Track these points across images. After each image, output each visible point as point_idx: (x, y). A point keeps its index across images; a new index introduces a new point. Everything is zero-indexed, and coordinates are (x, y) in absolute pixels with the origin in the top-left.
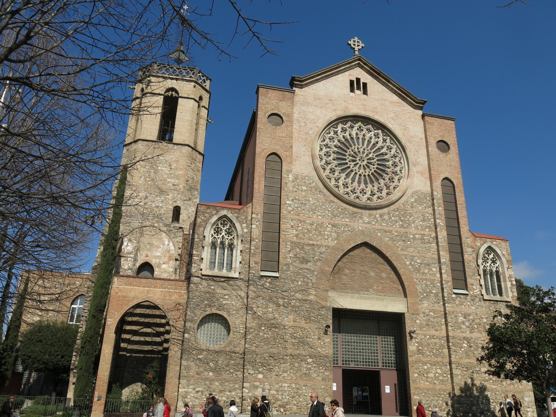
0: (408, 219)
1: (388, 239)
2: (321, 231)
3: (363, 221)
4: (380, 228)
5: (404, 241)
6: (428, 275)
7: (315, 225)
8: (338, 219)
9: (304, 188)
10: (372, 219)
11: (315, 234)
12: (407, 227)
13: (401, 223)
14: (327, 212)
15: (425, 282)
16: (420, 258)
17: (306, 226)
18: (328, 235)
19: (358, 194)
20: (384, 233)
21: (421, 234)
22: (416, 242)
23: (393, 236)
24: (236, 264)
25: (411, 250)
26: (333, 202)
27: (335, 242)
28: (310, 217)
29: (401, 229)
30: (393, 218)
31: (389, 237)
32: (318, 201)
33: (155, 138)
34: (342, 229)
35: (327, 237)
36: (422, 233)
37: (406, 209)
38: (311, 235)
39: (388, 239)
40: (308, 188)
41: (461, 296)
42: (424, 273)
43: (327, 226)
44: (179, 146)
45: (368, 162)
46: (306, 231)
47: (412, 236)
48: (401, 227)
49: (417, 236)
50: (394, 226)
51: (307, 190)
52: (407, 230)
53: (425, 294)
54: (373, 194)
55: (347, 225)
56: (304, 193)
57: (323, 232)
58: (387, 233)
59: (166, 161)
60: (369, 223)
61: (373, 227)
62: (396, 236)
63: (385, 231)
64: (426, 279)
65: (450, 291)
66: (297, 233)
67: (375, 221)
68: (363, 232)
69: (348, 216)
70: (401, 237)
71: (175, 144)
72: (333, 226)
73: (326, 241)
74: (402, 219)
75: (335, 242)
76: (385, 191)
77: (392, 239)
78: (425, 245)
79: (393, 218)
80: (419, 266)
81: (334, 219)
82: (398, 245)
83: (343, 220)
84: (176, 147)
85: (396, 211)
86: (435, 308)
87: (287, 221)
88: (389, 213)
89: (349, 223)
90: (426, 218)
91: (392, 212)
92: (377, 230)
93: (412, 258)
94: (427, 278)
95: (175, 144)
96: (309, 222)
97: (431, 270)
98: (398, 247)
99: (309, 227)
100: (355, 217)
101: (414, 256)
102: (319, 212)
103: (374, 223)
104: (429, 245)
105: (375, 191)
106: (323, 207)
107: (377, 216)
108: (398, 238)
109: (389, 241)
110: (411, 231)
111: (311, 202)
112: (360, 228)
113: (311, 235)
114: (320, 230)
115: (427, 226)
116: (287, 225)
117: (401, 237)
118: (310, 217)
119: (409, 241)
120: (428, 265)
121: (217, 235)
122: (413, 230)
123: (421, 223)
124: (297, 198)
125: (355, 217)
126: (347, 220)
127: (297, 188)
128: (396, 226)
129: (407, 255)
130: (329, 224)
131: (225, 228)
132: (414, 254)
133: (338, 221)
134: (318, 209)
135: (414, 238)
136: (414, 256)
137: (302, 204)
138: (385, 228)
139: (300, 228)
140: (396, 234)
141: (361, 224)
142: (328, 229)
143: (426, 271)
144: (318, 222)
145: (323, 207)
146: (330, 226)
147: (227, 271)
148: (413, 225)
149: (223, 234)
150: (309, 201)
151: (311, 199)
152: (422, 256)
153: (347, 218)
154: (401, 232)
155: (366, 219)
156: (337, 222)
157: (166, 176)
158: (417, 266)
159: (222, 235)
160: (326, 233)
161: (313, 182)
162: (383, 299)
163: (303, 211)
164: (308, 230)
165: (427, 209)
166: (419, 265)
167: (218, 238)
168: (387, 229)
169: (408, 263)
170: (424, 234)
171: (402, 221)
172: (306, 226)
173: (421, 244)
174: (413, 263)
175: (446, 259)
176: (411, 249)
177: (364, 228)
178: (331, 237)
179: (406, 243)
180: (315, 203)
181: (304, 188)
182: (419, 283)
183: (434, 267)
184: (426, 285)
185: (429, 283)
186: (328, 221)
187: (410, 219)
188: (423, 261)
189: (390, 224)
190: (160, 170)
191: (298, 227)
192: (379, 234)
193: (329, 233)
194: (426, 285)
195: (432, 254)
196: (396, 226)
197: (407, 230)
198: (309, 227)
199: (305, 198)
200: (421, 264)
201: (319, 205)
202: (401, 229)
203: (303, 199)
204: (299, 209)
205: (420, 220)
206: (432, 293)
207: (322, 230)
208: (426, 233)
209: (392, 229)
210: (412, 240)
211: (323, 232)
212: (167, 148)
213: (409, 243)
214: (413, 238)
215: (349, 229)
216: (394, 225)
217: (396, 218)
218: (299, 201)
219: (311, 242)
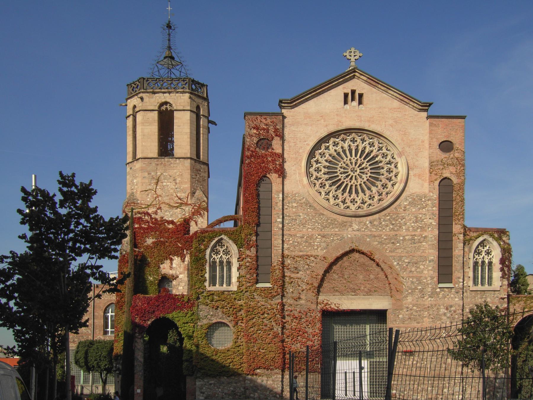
0: (400, 222)
1: (377, 243)
2: (310, 243)
3: (353, 229)
4: (369, 233)
5: (393, 243)
6: (415, 273)
7: (305, 237)
8: (327, 230)
9: (295, 205)
10: (361, 226)
11: (305, 246)
12: (398, 230)
13: (391, 227)
14: (317, 224)
15: (411, 279)
16: (408, 257)
17: (297, 240)
18: (317, 245)
19: (349, 204)
20: (373, 238)
21: (411, 235)
22: (405, 243)
23: (383, 239)
24: (234, 279)
25: (399, 251)
26: (323, 214)
27: (325, 251)
28: (300, 231)
29: (391, 233)
30: (383, 223)
31: (378, 241)
32: (308, 215)
33: (156, 155)
34: (332, 239)
35: (316, 247)
36: (413, 233)
37: (397, 212)
38: (301, 247)
39: (377, 243)
40: (299, 204)
41: (445, 289)
42: (411, 271)
43: (317, 238)
44: (181, 159)
45: (360, 169)
46: (296, 244)
47: (401, 238)
48: (390, 231)
49: (407, 238)
50: (384, 231)
51: (297, 206)
52: (397, 233)
53: (410, 291)
54: (363, 203)
55: (336, 234)
56: (294, 210)
57: (313, 243)
58: (377, 238)
59: (171, 176)
60: (358, 231)
61: (363, 233)
62: (386, 239)
63: (375, 236)
64: (413, 277)
65: (434, 287)
66: (288, 246)
67: (365, 227)
68: (352, 240)
69: (337, 226)
70: (391, 239)
71: (177, 158)
72: (323, 237)
73: (316, 250)
74: (393, 222)
75: (325, 251)
76: (377, 198)
77: (381, 243)
78: (415, 245)
79: (383, 223)
80: (407, 265)
81: (323, 230)
82: (386, 247)
83: (333, 230)
84: (178, 161)
85: (387, 216)
86: (419, 303)
87: (278, 237)
88: (380, 219)
89: (338, 233)
90: (419, 218)
91: (383, 217)
92: (367, 236)
93: (400, 258)
94: (414, 275)
95: (177, 158)
96: (300, 235)
97: (419, 268)
98: (386, 250)
99: (299, 240)
100: (345, 226)
101: (403, 257)
102: (309, 225)
103: (363, 230)
104: (420, 244)
105: (367, 199)
106: (313, 220)
107: (367, 222)
108: (387, 241)
109: (377, 244)
110: (402, 233)
111: (302, 217)
112: (349, 236)
113: (301, 247)
114: (310, 241)
115: (419, 226)
116: (279, 241)
117: (391, 239)
118: (300, 231)
119: (398, 243)
120: (416, 264)
121: (217, 256)
122: (404, 232)
123: (413, 224)
124: (288, 215)
125: (345, 226)
126: (337, 230)
127: (288, 206)
128: (386, 230)
129: (395, 256)
130: (319, 235)
131: (223, 249)
132: (403, 255)
133: (327, 231)
134: (308, 223)
135: (404, 240)
136: (403, 257)
137: (292, 220)
138: (374, 233)
139: (291, 242)
140: (385, 237)
141: (351, 232)
142: (318, 240)
143: (413, 269)
144: (308, 234)
145: (313, 220)
146: (320, 237)
147: (227, 286)
148: (404, 227)
149: (221, 254)
150: (300, 216)
151: (301, 214)
152: (411, 256)
153: (337, 228)
154: (391, 235)
155: (355, 227)
156: (327, 233)
157: (172, 191)
158: (405, 265)
159: (220, 256)
160: (316, 243)
161: (303, 198)
162: (369, 298)
163: (294, 226)
164: (298, 243)
165: (420, 210)
166: (407, 264)
167: (218, 258)
168: (376, 234)
169: (395, 263)
170: (415, 235)
171: (393, 224)
172: (297, 240)
173: (411, 244)
174: (400, 263)
175: (434, 257)
176: (399, 250)
177: (353, 236)
178: (321, 246)
179: (395, 245)
180: (305, 218)
181: (295, 205)
182: (405, 281)
183: (422, 265)
184: (412, 282)
185: (415, 280)
186: (318, 232)
187: (401, 222)
188: (411, 260)
189: (380, 229)
190: (165, 186)
191: (289, 241)
192: (368, 240)
193: (319, 244)
194: (412, 282)
195: (422, 252)
196: (386, 230)
197: (397, 233)
198: (299, 240)
199: (295, 214)
200: (409, 263)
201: (309, 219)
202: (391, 233)
203: (293, 215)
204: (290, 224)
205: (412, 222)
206: (417, 289)
207: (312, 241)
208: (416, 233)
209: (381, 233)
210: (401, 242)
211: (313, 243)
212: (169, 163)
213: (398, 244)
214: (402, 240)
215: (338, 238)
216: (384, 229)
217: (387, 222)
218: (290, 217)
219: (301, 253)
